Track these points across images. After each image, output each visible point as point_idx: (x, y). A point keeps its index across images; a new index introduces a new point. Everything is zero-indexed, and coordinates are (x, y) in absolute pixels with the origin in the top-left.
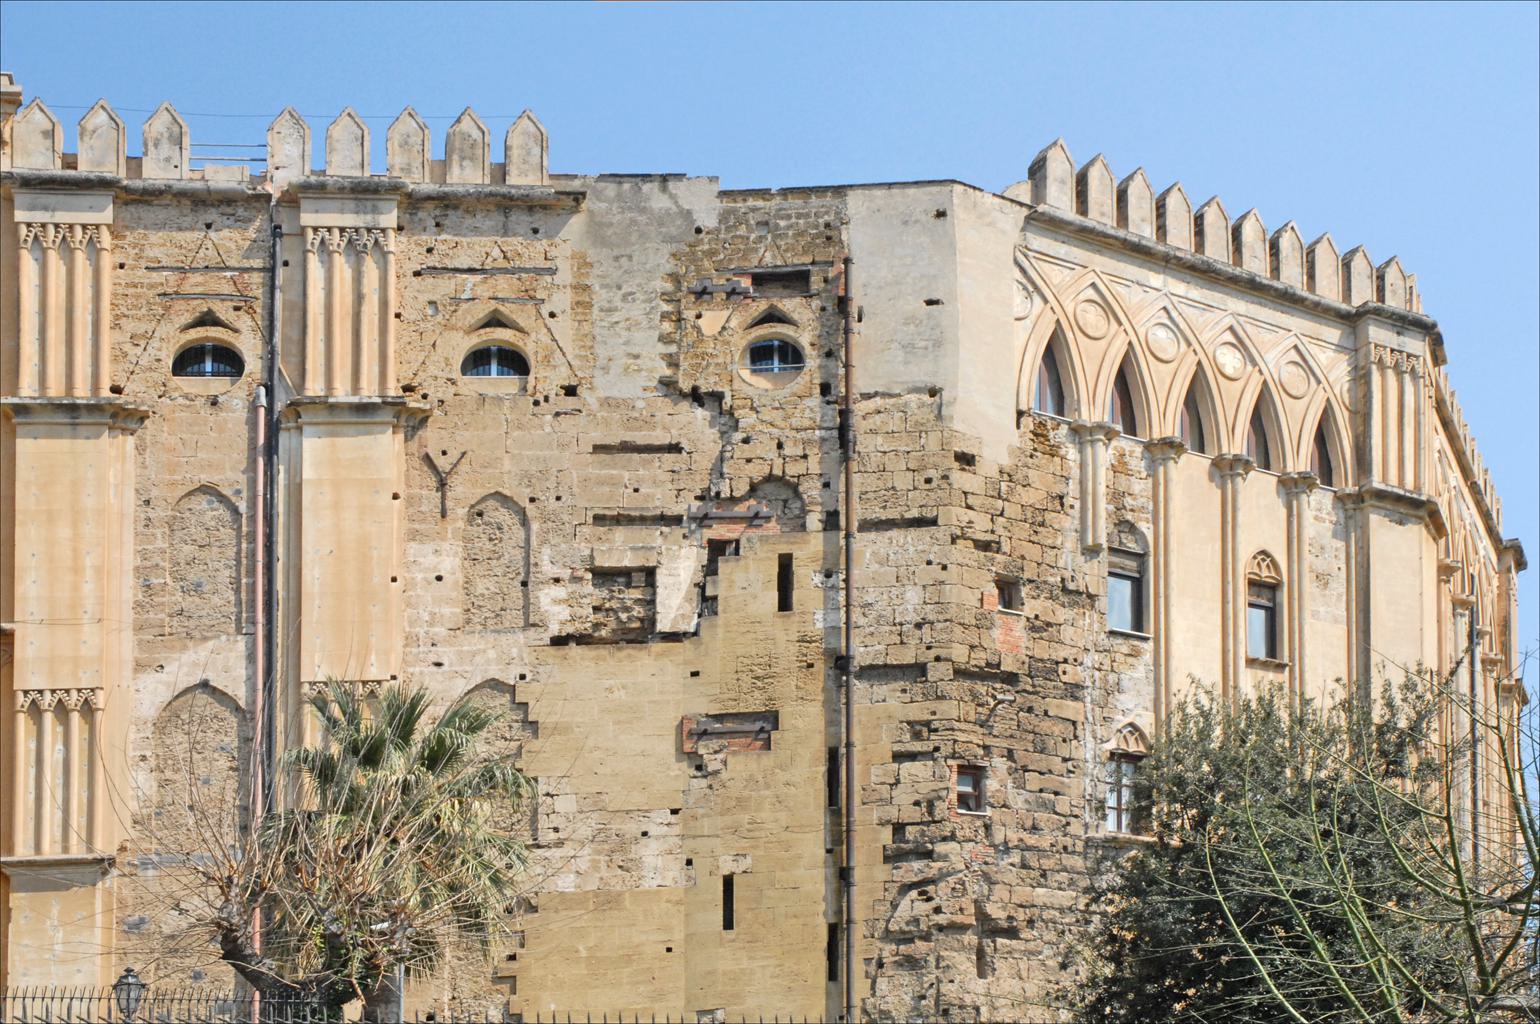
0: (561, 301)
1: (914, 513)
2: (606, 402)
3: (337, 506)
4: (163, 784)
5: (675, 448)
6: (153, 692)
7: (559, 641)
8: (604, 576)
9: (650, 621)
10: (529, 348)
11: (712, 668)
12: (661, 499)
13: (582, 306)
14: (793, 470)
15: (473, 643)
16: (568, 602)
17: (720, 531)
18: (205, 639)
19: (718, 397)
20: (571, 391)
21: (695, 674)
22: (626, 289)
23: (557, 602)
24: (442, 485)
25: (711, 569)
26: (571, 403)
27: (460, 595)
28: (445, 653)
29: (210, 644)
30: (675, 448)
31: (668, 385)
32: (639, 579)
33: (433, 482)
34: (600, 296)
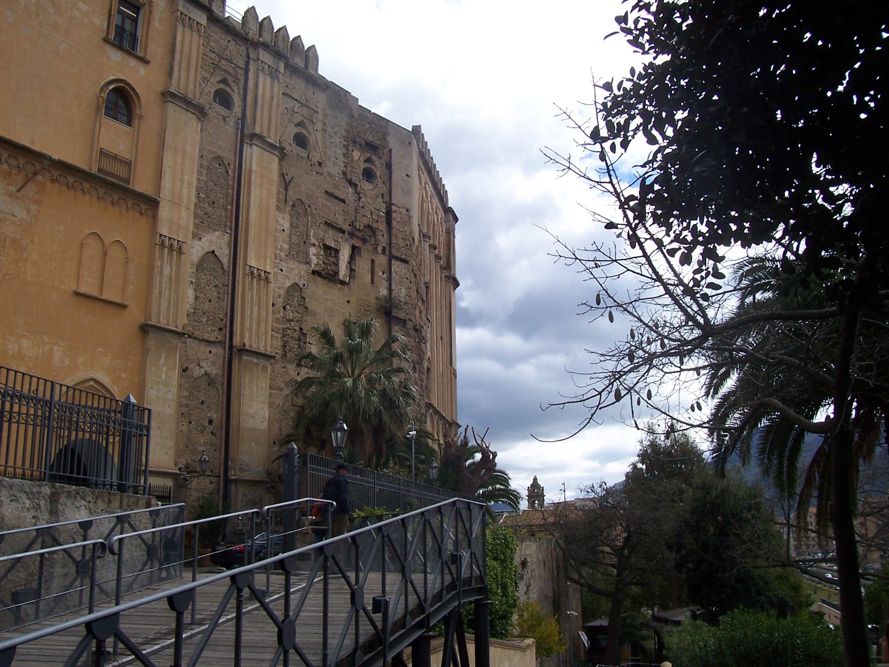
0: (319, 126)
1: (403, 257)
2: (329, 173)
3: (261, 186)
4: (196, 298)
5: (343, 201)
6: (196, 250)
7: (314, 272)
8: (327, 248)
9: (337, 273)
10: (312, 139)
11: (354, 300)
12: (340, 220)
13: (324, 130)
14: (375, 225)
15: (292, 264)
16: (317, 255)
17: (358, 243)
18: (215, 230)
19: (356, 185)
20: (320, 164)
21: (348, 302)
22: (335, 130)
23: (314, 255)
24: (286, 189)
25: (352, 258)
26: (319, 170)
27: (288, 239)
28: (284, 265)
29: (217, 233)
30: (343, 201)
31: (344, 173)
32: (333, 254)
33: (283, 185)
34: (329, 129)
